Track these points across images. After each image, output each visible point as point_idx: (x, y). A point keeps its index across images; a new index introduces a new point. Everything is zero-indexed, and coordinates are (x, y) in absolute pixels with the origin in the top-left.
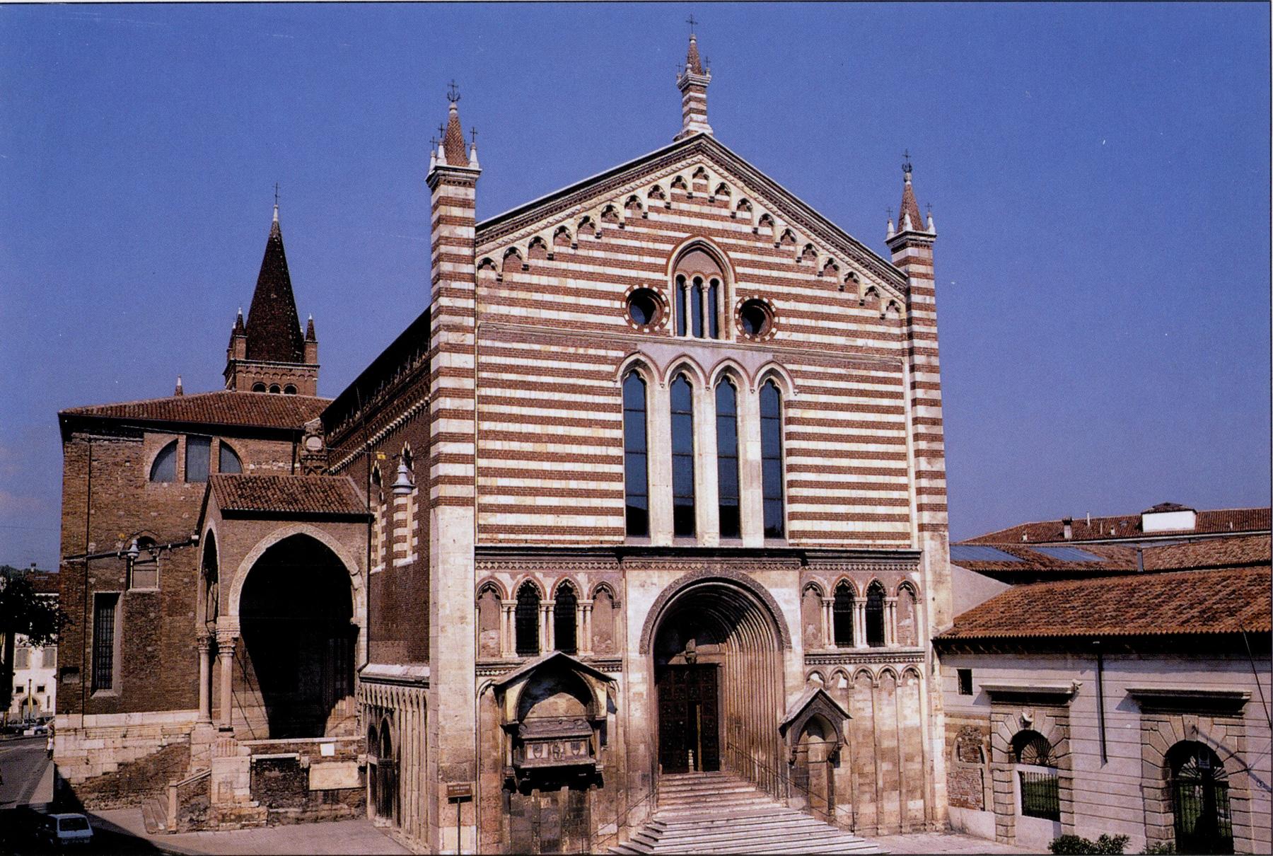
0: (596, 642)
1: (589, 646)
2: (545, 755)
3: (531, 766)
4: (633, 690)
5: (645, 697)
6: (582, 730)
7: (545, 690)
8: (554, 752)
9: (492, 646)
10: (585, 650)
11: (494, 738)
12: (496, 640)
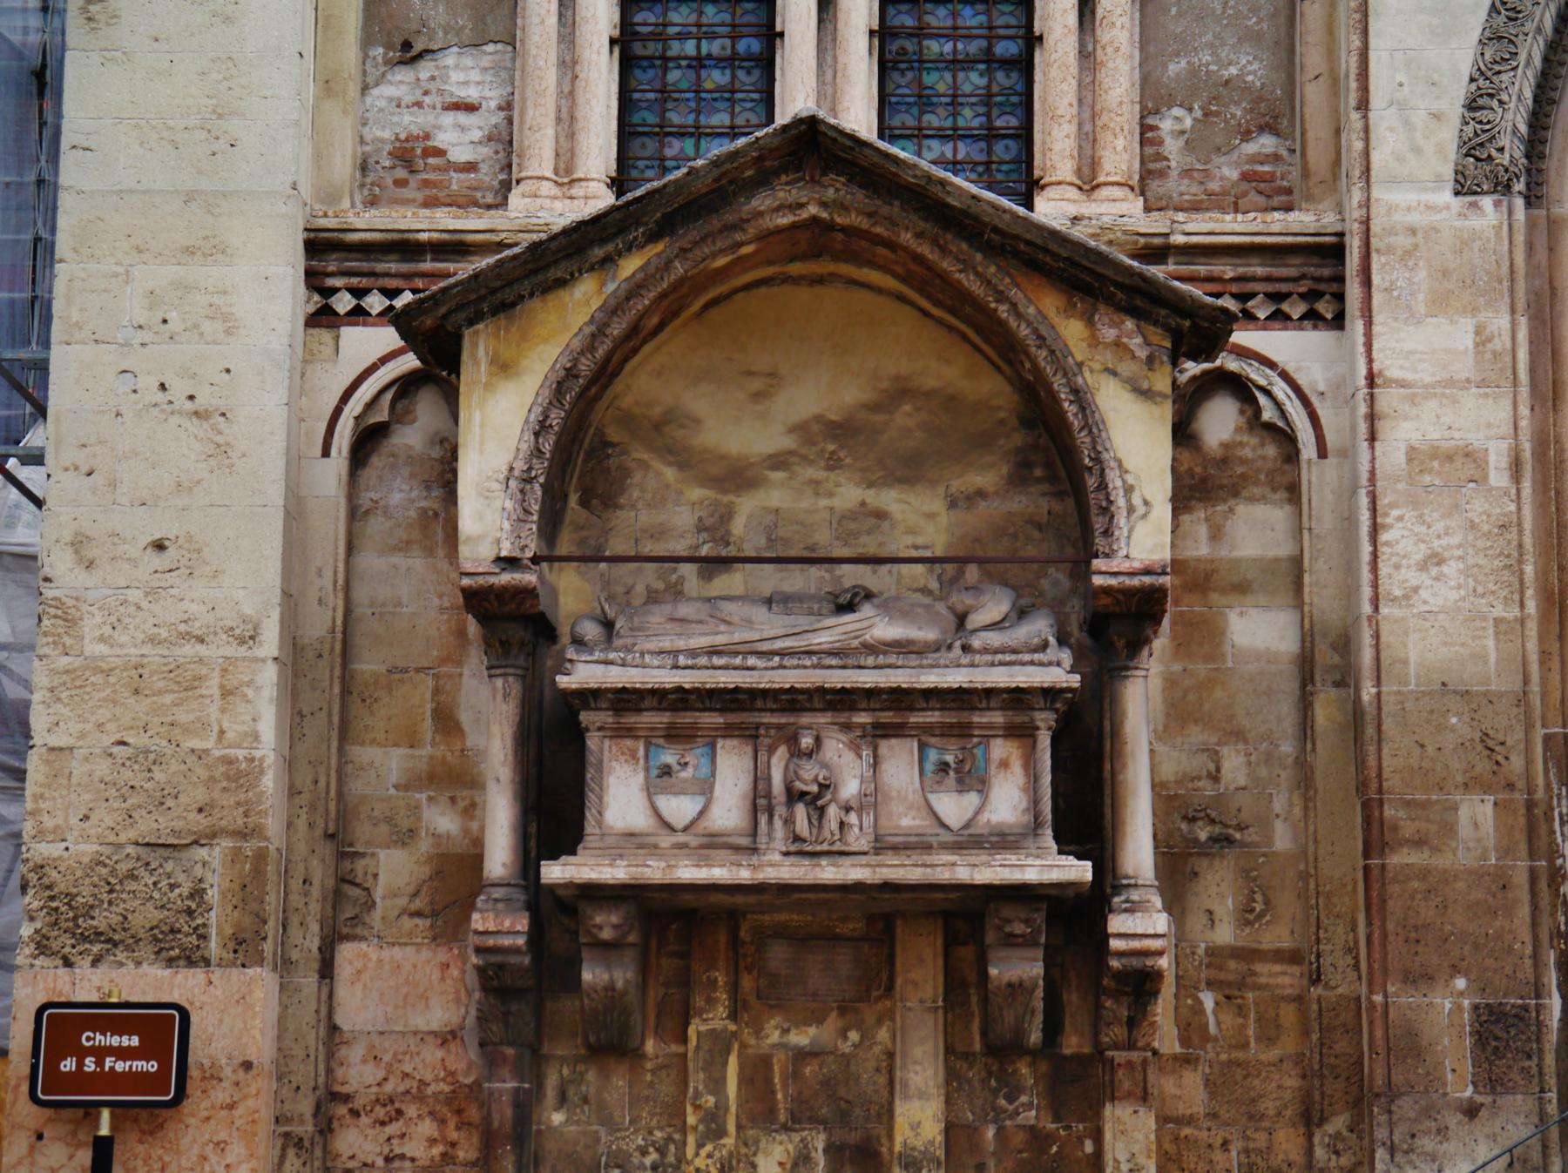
0: (1172, 147)
1: (1119, 156)
2: (728, 811)
3: (616, 873)
4: (1400, 436)
5: (1499, 477)
6: (1010, 655)
7: (800, 429)
8: (794, 796)
9: (459, 155)
10: (1089, 183)
11: (446, 722)
12: (487, 119)
